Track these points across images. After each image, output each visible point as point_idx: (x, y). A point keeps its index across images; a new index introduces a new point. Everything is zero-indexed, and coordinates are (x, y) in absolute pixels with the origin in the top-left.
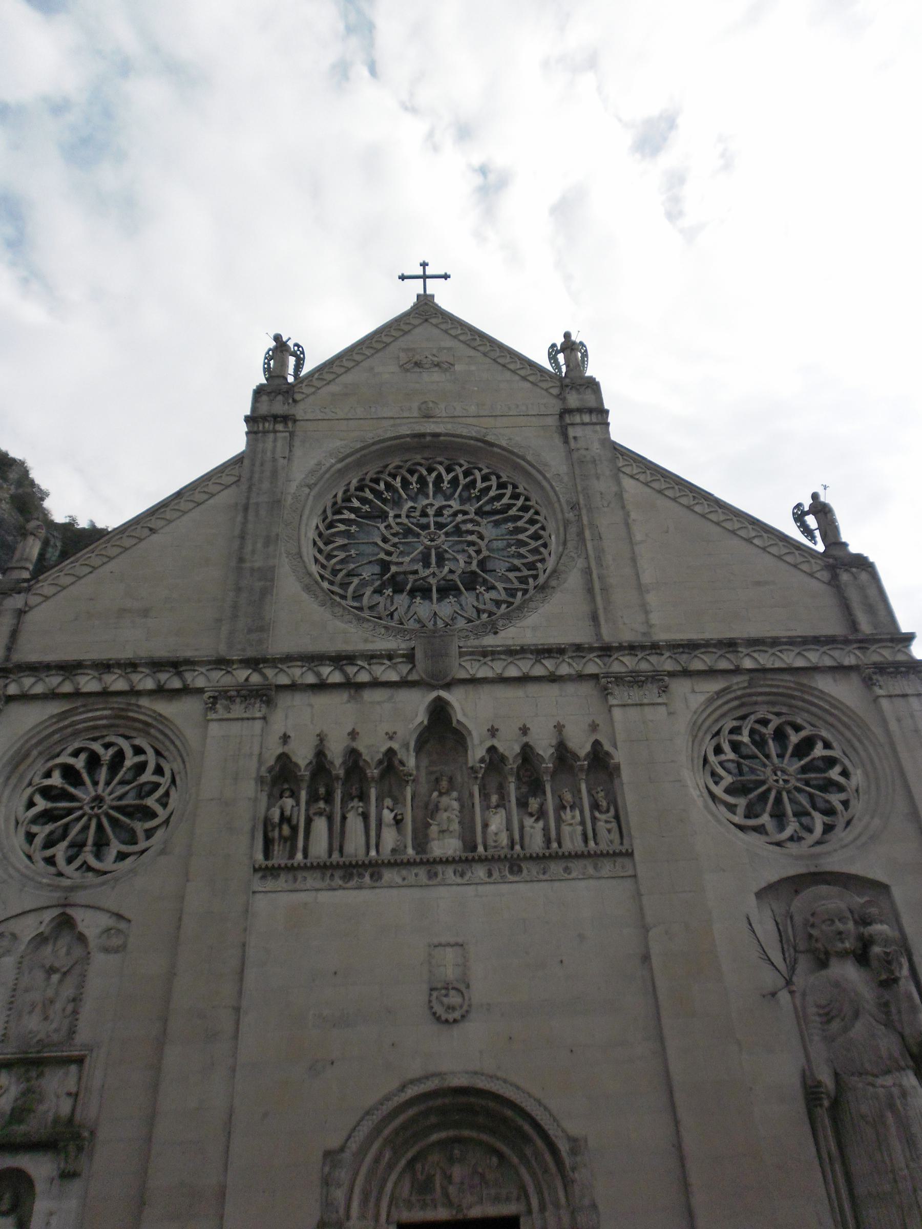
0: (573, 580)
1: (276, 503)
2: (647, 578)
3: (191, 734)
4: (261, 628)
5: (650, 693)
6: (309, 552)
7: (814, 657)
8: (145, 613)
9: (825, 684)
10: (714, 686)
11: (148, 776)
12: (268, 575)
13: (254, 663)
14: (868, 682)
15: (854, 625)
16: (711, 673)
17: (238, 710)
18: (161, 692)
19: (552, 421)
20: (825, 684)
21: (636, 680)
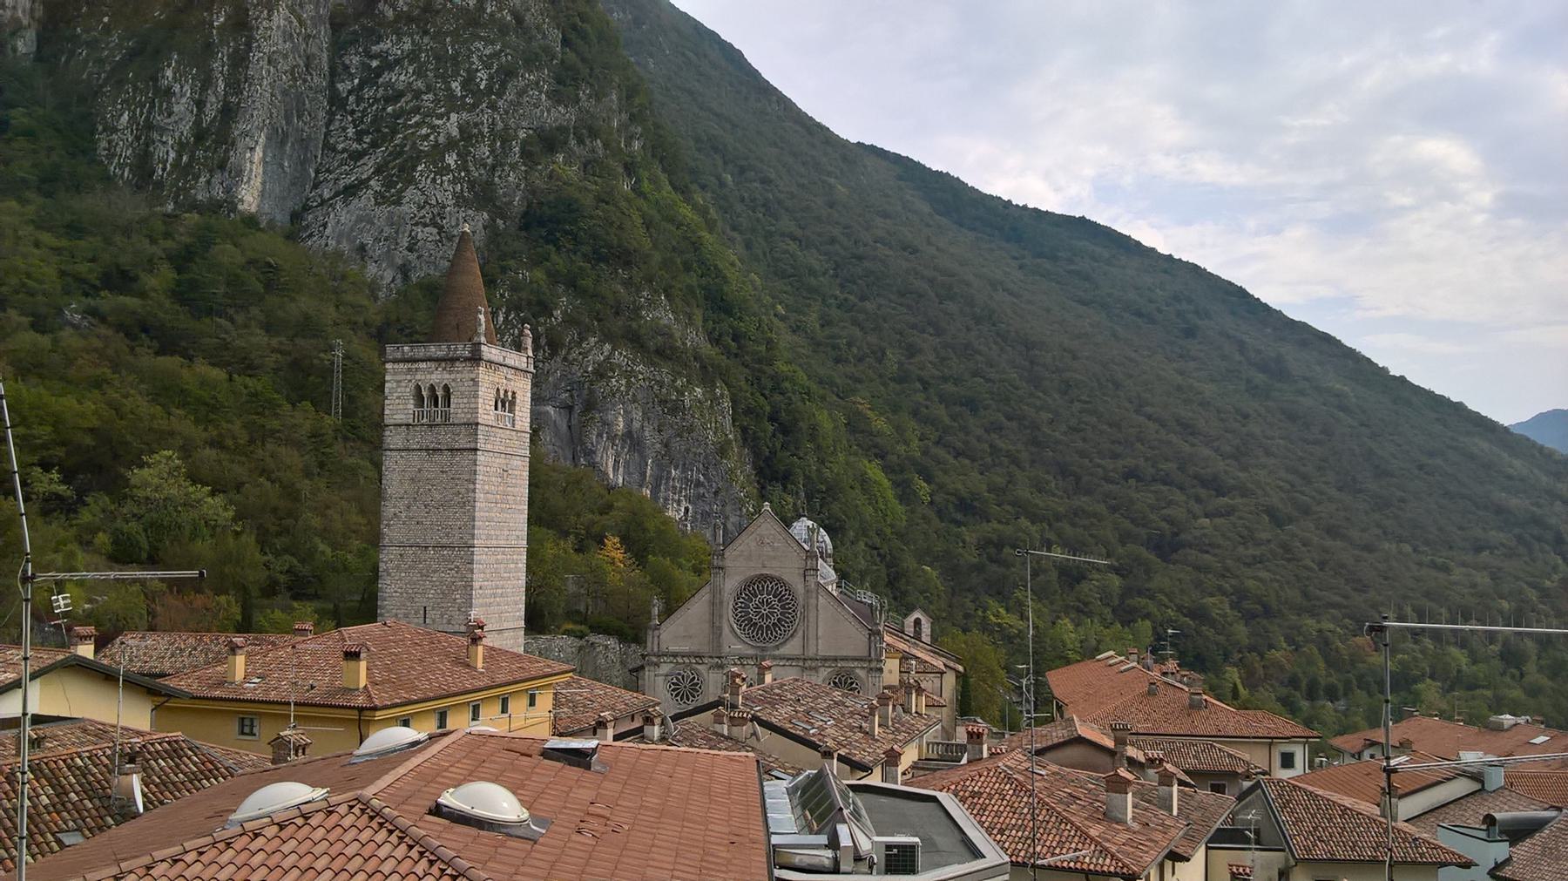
0: (800, 633)
1: (721, 603)
2: (820, 634)
3: (705, 674)
4: (720, 646)
5: (813, 673)
6: (730, 612)
7: (856, 664)
8: (691, 637)
9: (858, 671)
10: (830, 670)
11: (696, 681)
12: (720, 628)
13: (719, 658)
14: (868, 672)
15: (870, 655)
16: (830, 667)
17: (716, 670)
18: (697, 663)
19: (802, 571)
20: (858, 671)
21: (811, 668)
